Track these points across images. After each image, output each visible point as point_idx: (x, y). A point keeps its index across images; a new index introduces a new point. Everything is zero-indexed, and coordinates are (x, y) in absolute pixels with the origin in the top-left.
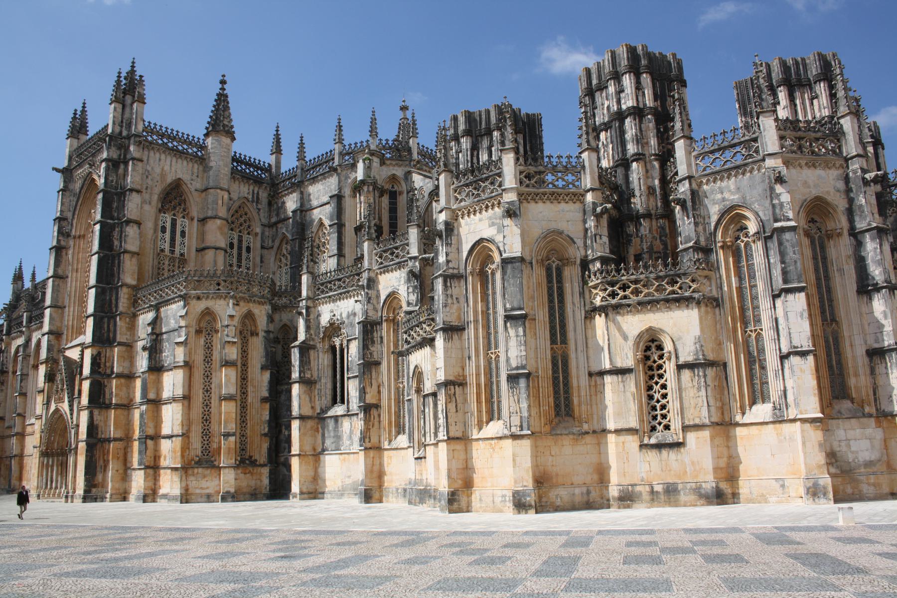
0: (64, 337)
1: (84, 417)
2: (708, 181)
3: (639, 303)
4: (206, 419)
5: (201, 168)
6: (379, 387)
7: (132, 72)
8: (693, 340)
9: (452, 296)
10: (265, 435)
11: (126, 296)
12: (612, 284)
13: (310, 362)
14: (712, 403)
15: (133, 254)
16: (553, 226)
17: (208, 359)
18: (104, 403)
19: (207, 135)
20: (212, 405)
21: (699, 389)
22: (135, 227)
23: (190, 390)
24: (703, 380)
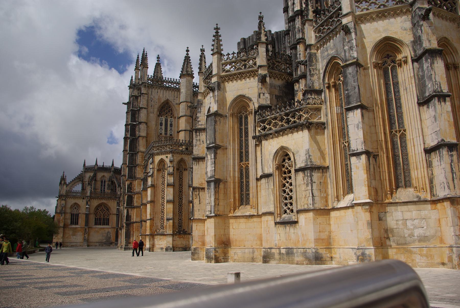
1: (125, 211)
2: (321, 45)
3: (276, 132)
5: (178, 93)
7: (143, 54)
8: (305, 153)
9: (200, 140)
12: (263, 122)
14: (316, 193)
15: (143, 137)
16: (240, 93)
19: (180, 77)
21: (307, 185)
24: (310, 179)
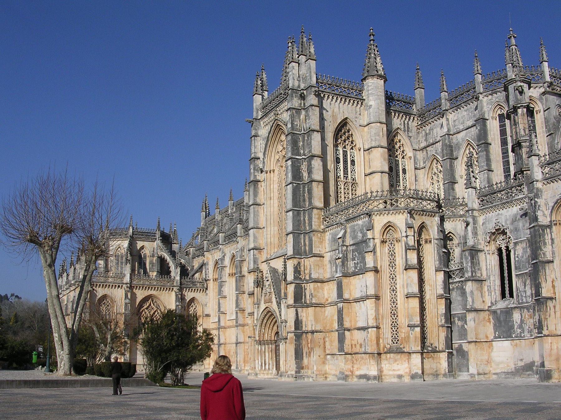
0: (265, 251)
4: (394, 314)
6: (552, 282)
10: (442, 326)
11: (317, 216)
13: (479, 264)
17: (392, 264)
18: (306, 303)
20: (399, 302)
22: (319, 159)
23: (379, 290)
